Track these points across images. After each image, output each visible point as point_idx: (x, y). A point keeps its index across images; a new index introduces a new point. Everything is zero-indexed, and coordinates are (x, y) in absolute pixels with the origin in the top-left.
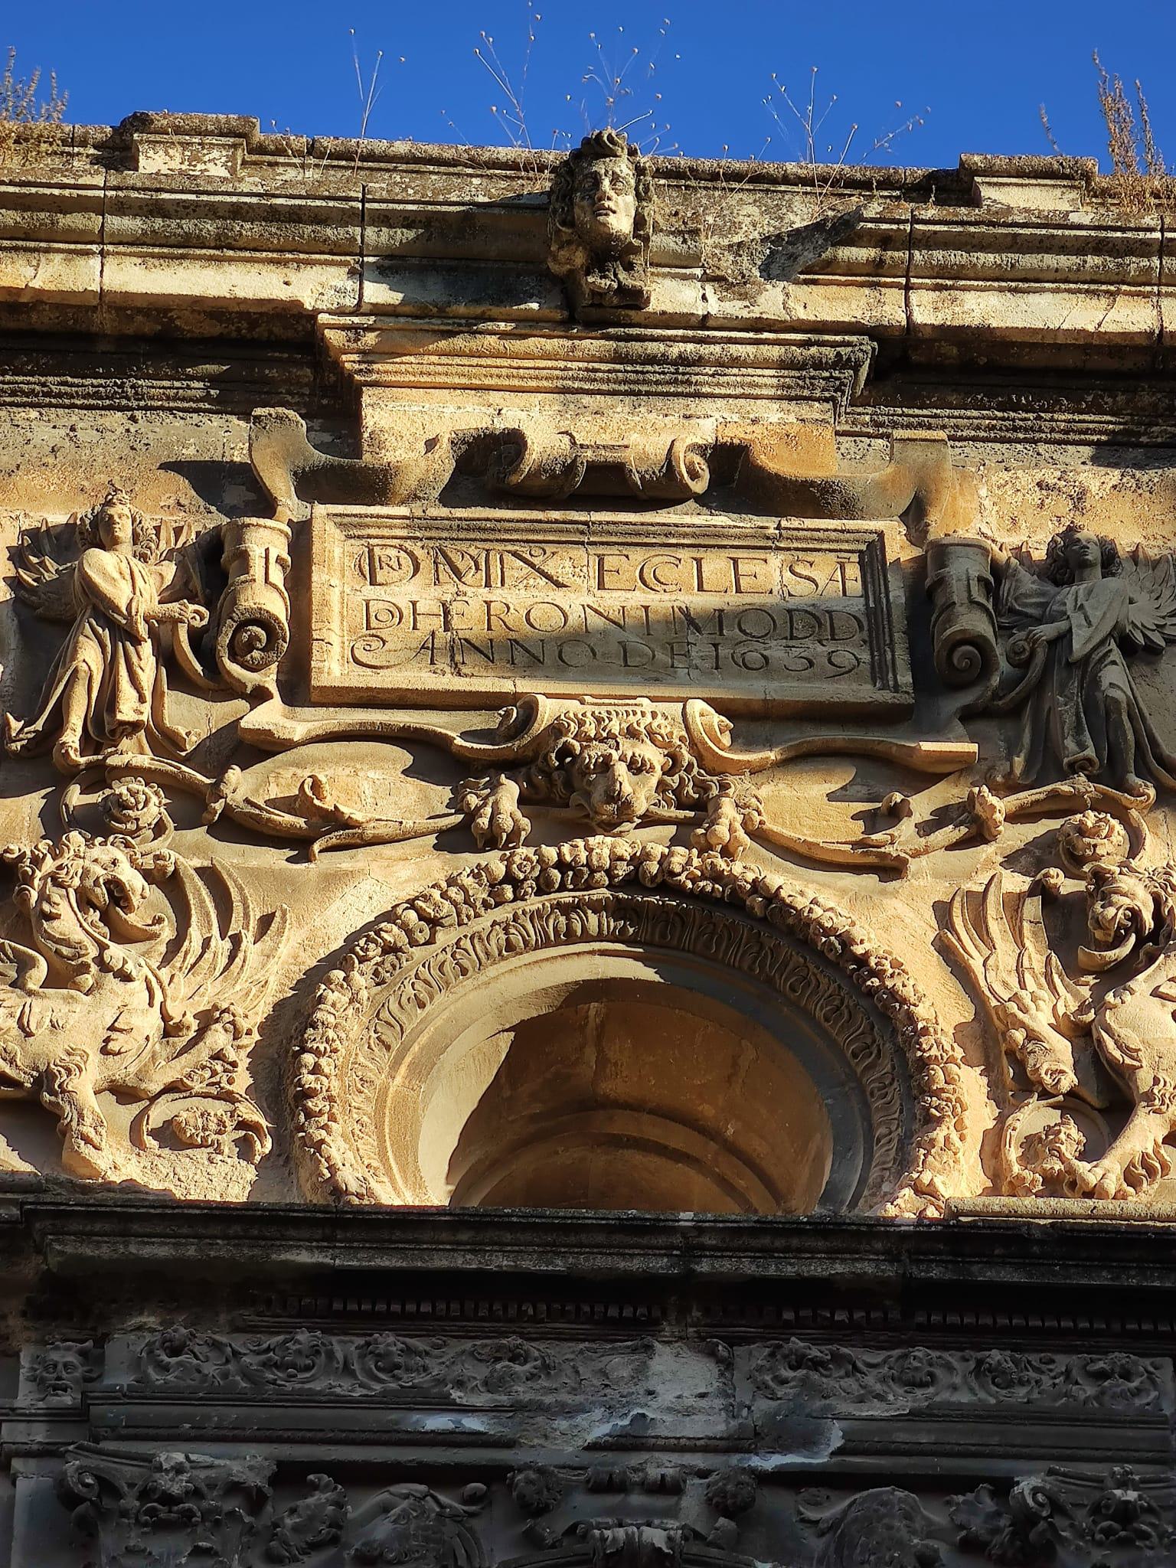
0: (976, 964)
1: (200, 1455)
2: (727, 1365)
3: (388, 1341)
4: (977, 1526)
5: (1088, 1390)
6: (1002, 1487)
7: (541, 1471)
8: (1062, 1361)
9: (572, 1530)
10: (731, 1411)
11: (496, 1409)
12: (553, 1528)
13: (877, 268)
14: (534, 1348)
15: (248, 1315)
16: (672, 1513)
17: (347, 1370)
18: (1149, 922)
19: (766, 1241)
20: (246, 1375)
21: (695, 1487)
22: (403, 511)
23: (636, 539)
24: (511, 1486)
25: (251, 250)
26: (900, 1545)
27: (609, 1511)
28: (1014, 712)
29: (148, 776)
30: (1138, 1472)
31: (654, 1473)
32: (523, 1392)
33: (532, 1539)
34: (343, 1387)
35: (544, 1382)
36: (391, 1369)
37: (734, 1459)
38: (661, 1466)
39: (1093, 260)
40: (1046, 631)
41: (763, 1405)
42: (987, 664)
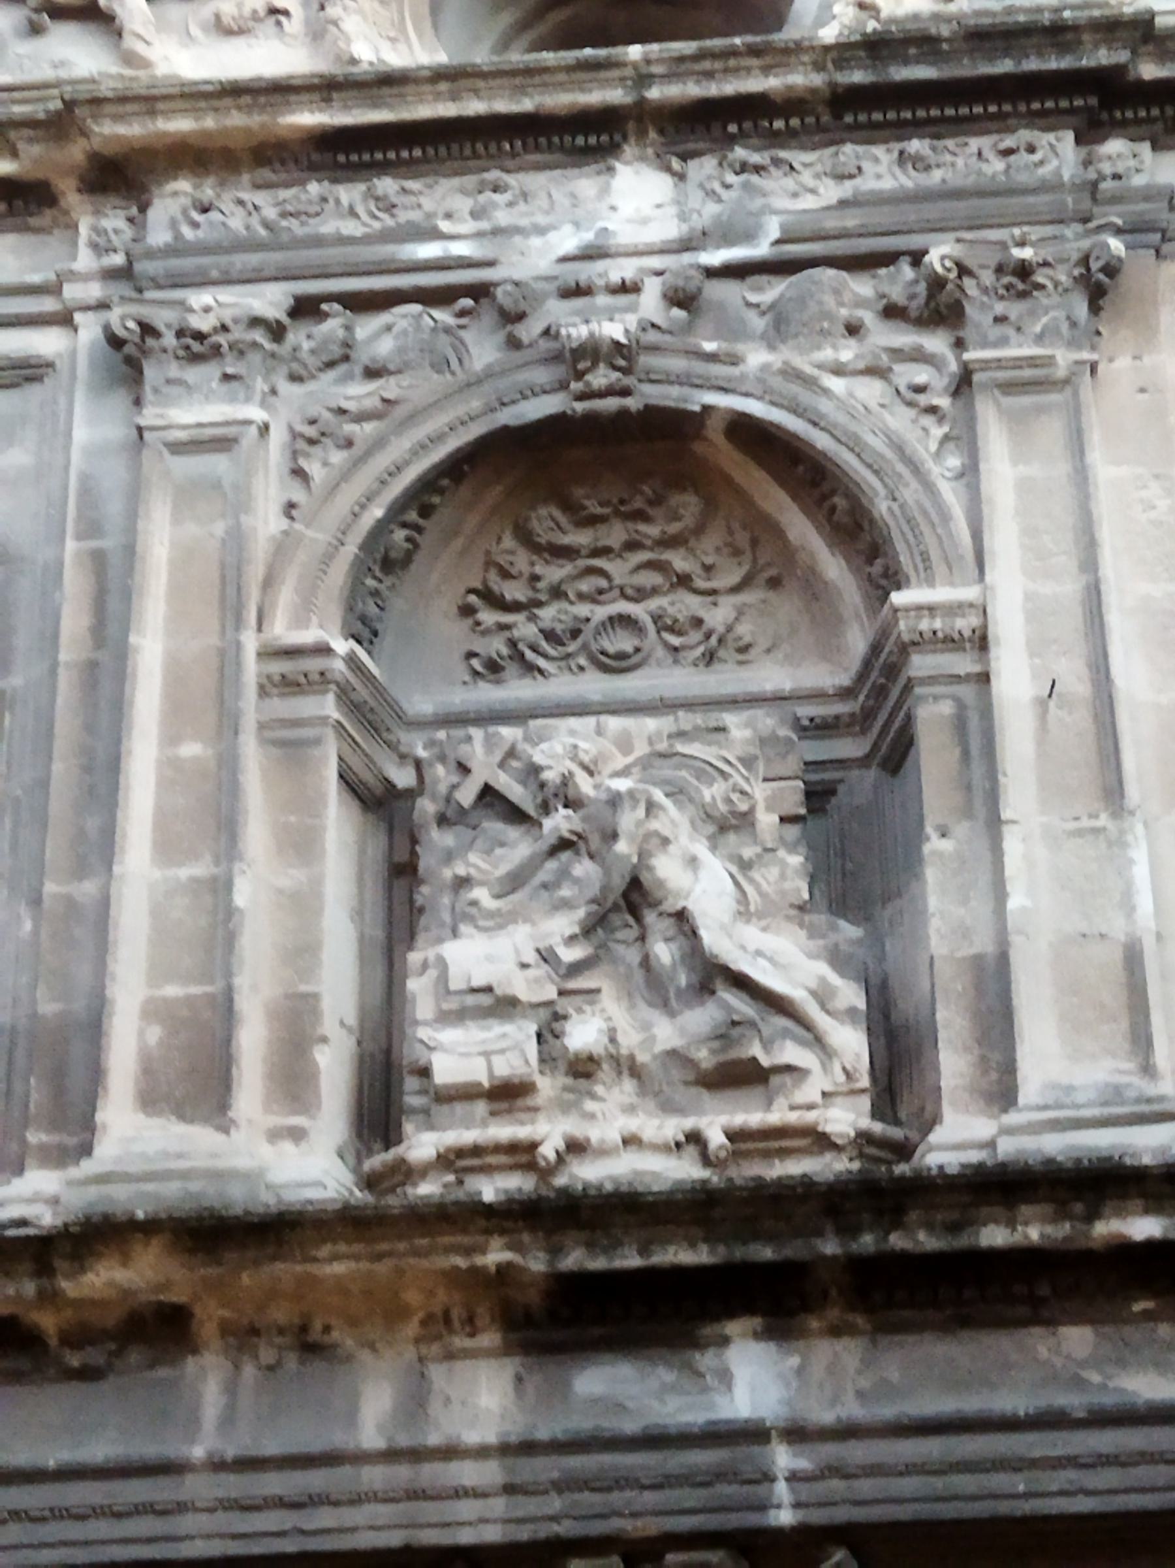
7: (517, 284)
9: (547, 332)
10: (683, 217)
11: (479, 235)
14: (511, 180)
15: (266, 174)
16: (632, 308)
17: (352, 213)
19: (707, 65)
20: (267, 225)
24: (494, 298)
26: (828, 315)
27: (577, 313)
31: (615, 277)
35: (522, 207)
36: (390, 208)
37: (687, 258)
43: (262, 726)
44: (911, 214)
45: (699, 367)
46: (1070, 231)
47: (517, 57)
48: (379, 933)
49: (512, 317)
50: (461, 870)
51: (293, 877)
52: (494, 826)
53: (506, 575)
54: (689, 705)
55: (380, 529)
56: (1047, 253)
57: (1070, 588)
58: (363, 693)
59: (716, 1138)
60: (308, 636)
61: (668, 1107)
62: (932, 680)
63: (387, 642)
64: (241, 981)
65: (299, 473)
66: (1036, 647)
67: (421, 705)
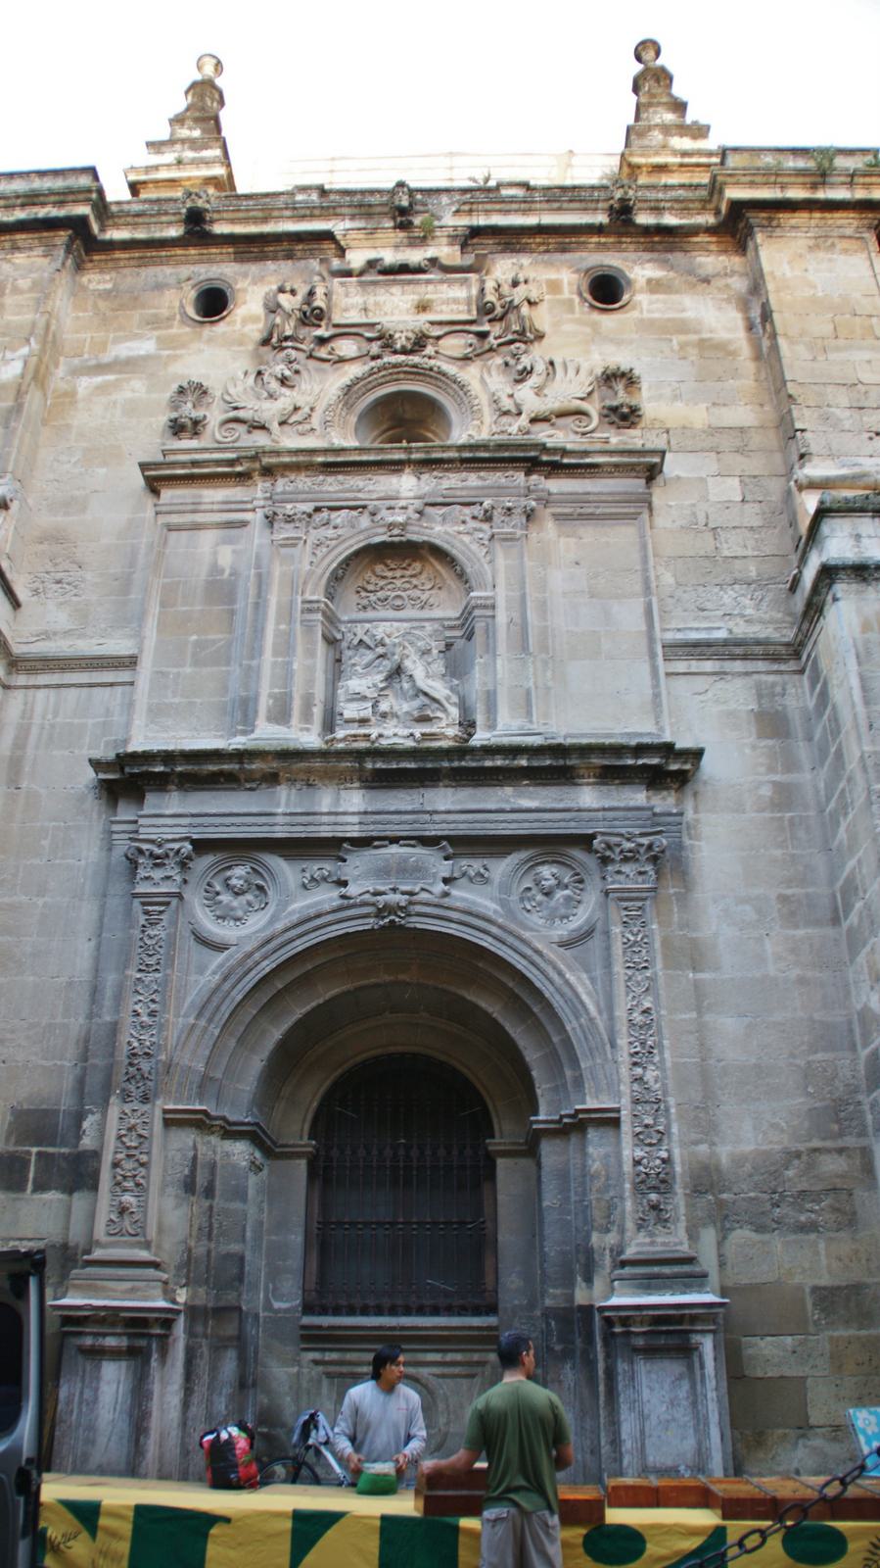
0: (488, 380)
1: (298, 505)
2: (419, 478)
3: (340, 477)
4: (476, 513)
5: (503, 480)
6: (481, 504)
8: (498, 474)
12: (378, 517)
13: (471, 211)
18: (529, 368)
21: (411, 508)
22: (355, 279)
23: (410, 282)
25: (319, 217)
28: (501, 319)
29: (293, 348)
30: (513, 499)
32: (371, 488)
33: (373, 521)
34: (330, 489)
38: (403, 503)
39: (523, 206)
40: (508, 299)
41: (427, 488)
42: (493, 309)
43: (302, 621)
44: (480, 492)
45: (422, 530)
46: (523, 499)
47: (376, 445)
48: (330, 677)
49: (373, 514)
50: (353, 661)
51: (309, 662)
52: (362, 650)
53: (368, 583)
54: (416, 620)
55: (335, 570)
56: (516, 504)
57: (517, 594)
58: (329, 613)
59: (418, 735)
60: (315, 598)
61: (406, 727)
62: (480, 617)
63: (336, 600)
64: (295, 689)
65: (314, 553)
66: (508, 609)
67: (345, 618)
